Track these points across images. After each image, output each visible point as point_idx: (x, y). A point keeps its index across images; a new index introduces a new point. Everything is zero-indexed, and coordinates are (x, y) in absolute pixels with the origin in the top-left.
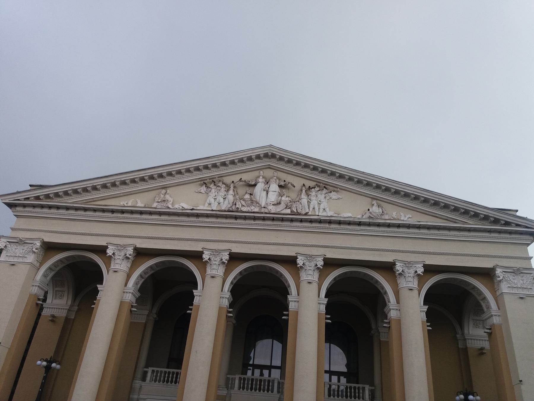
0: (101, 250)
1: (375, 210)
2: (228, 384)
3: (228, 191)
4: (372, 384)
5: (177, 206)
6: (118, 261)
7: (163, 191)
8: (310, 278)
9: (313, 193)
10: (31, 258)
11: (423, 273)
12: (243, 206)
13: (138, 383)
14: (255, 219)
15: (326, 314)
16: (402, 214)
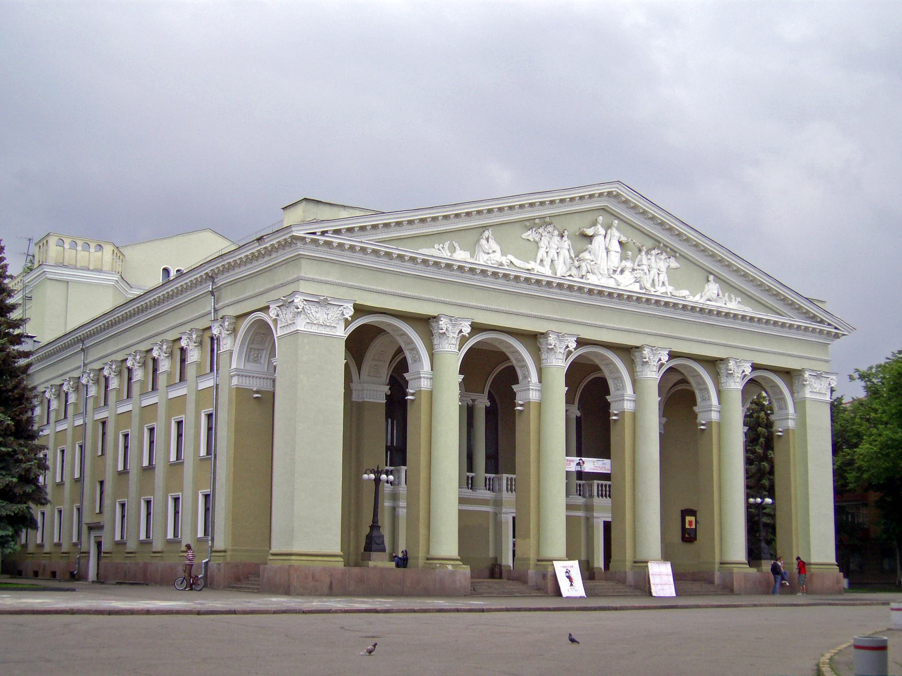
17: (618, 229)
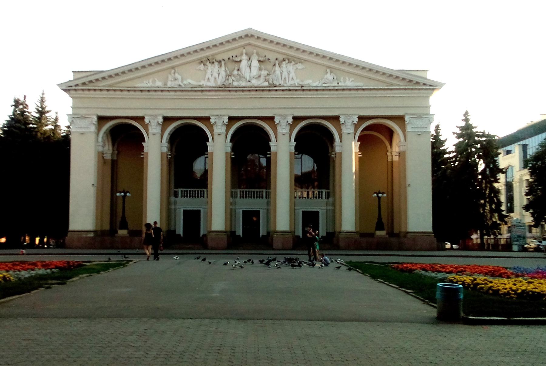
0: (141, 119)
1: (329, 76)
2: (233, 195)
3: (221, 66)
4: (328, 188)
5: (185, 82)
6: (153, 127)
7: (173, 71)
8: (284, 131)
9: (284, 64)
10: (93, 129)
11: (358, 122)
12: (233, 81)
13: (173, 199)
14: (243, 91)
15: (295, 151)
16: (347, 78)
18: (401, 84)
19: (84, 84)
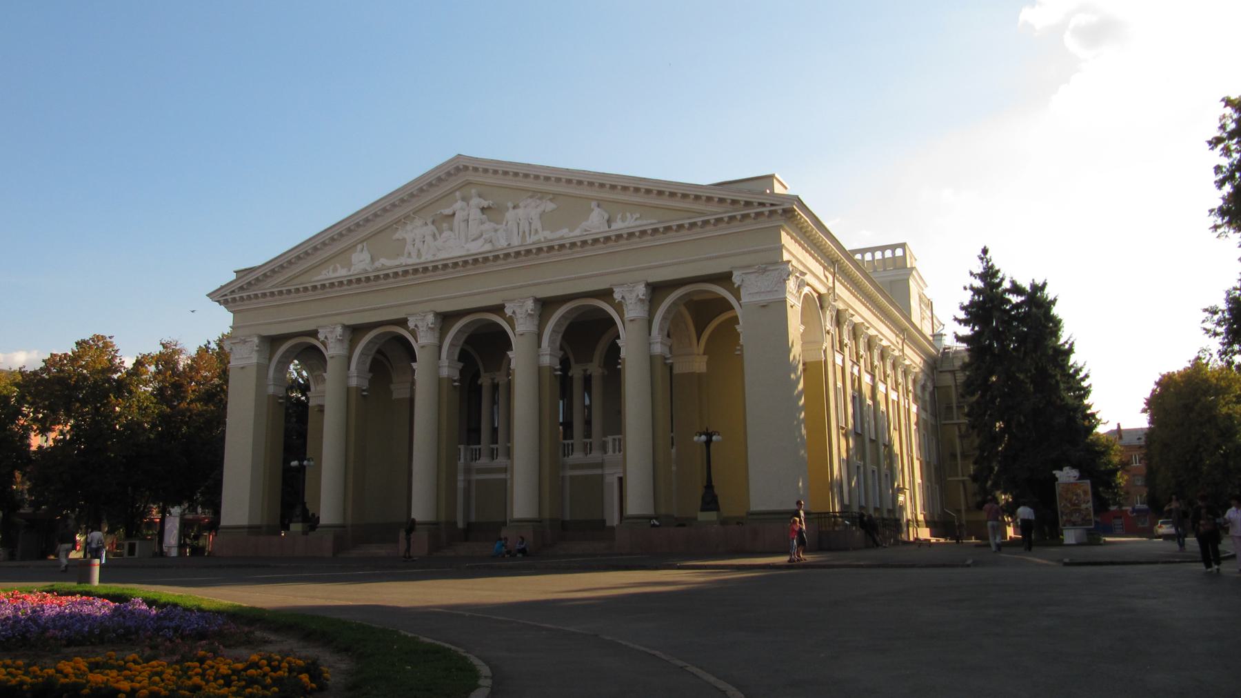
10: (254, 359)
16: (628, 215)
17: (480, 196)
18: (720, 210)
19: (241, 288)
